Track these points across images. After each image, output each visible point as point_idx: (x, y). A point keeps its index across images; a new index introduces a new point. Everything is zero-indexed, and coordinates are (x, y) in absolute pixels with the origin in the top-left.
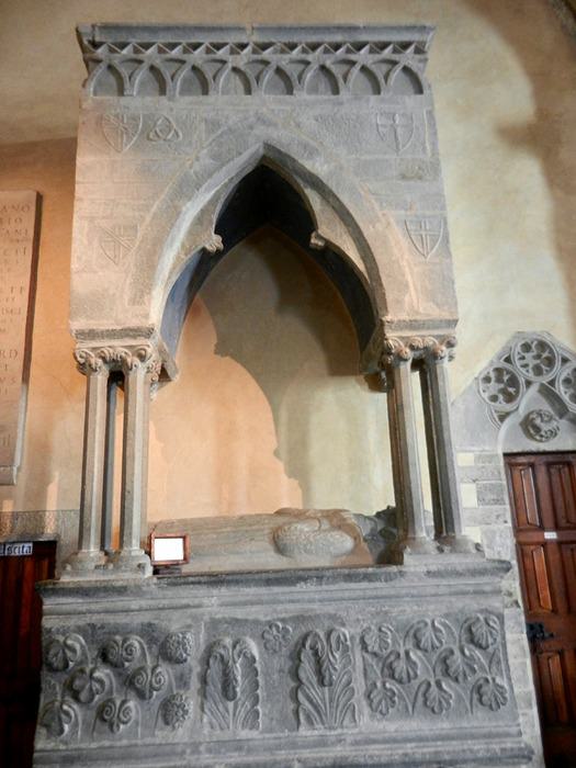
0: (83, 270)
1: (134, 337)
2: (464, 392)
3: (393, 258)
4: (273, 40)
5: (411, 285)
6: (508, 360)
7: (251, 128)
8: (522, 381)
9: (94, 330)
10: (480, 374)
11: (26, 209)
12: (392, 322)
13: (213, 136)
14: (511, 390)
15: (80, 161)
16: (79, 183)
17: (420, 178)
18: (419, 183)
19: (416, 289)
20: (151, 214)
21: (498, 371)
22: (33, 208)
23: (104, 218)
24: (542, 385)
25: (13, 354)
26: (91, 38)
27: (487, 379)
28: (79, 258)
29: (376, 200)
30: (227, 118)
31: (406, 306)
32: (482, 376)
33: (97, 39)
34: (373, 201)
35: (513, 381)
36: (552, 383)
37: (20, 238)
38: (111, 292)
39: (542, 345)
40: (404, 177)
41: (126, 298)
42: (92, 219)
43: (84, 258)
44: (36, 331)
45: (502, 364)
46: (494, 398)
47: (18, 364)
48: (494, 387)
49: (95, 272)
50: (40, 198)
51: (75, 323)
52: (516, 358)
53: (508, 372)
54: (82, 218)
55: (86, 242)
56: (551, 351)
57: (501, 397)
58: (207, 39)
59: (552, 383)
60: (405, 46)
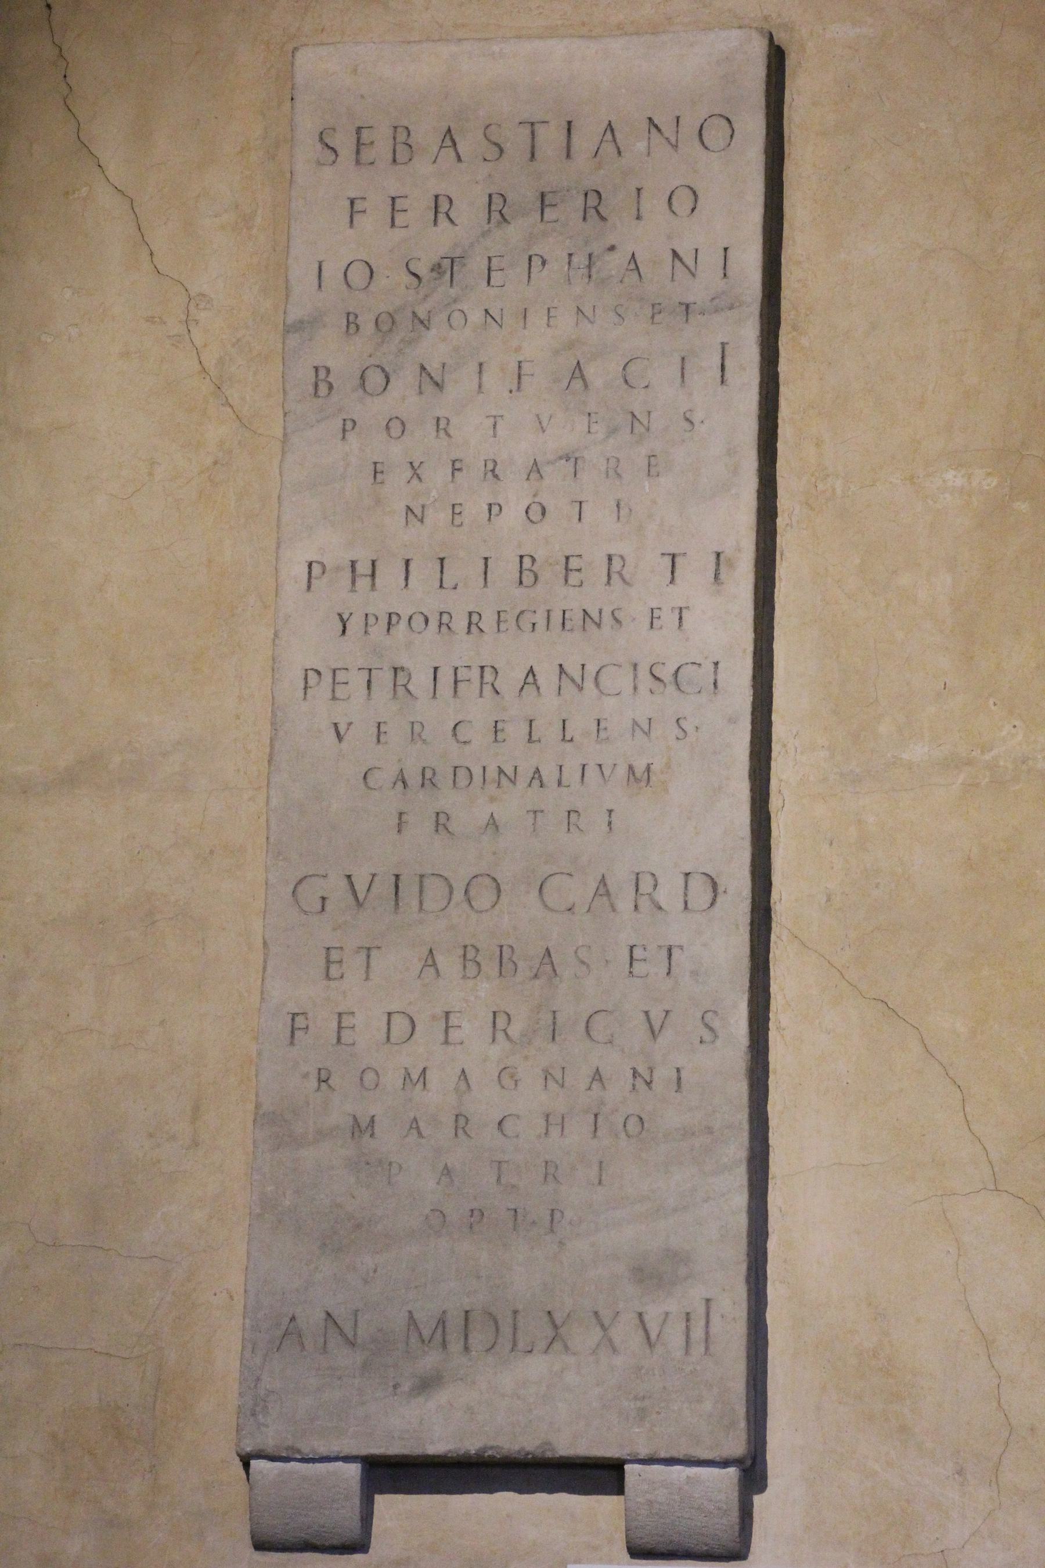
11: (716, 134)
22: (753, 126)
37: (697, 292)
47: (728, 945)
50: (777, 60)
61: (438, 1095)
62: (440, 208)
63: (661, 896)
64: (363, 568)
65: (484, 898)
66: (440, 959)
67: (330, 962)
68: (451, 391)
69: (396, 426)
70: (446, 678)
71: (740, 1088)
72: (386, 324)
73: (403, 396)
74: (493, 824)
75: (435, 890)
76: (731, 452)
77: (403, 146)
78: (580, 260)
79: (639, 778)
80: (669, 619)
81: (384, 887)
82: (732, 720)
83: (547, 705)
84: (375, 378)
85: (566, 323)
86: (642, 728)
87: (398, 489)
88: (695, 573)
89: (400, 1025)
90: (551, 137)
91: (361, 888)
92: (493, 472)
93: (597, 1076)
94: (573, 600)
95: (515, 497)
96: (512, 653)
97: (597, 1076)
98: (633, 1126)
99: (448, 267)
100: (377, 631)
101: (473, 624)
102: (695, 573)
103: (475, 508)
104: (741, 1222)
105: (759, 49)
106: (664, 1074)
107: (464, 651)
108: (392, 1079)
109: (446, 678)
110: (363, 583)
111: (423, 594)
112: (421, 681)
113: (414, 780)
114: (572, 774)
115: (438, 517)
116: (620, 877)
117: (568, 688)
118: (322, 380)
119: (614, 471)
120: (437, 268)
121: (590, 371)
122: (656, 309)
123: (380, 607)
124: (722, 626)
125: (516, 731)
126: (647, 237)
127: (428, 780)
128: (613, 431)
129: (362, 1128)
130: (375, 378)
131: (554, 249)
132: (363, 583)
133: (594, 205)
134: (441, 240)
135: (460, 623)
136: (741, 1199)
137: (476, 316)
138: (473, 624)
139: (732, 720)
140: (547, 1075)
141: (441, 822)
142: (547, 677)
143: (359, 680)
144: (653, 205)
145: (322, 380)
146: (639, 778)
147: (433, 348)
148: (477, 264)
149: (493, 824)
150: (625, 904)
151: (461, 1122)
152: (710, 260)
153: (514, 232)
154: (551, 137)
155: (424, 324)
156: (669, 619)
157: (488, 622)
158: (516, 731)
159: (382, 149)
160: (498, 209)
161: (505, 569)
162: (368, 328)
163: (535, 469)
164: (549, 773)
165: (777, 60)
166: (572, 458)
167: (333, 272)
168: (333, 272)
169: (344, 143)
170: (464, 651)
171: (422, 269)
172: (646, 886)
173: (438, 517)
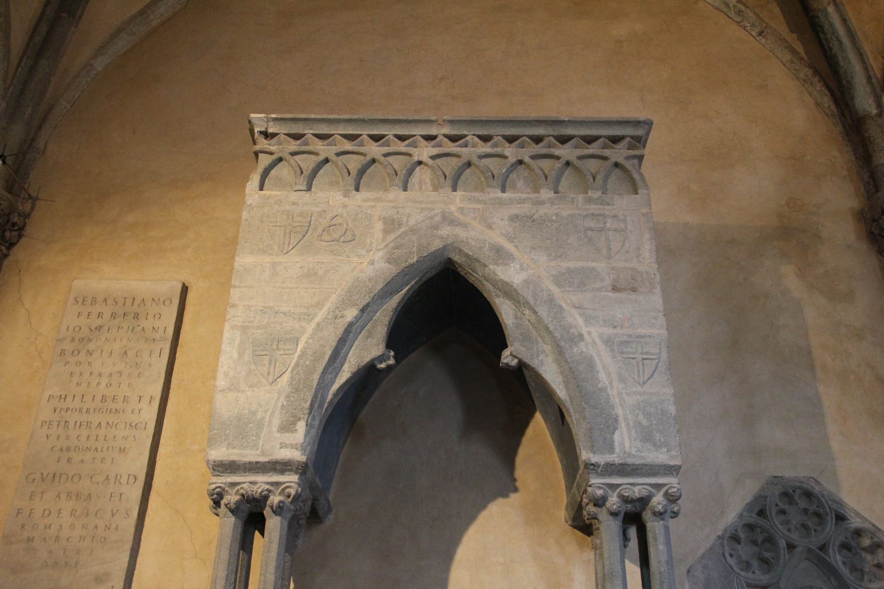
0: (230, 389)
1: (282, 472)
2: (703, 557)
3: (600, 386)
4: (466, 133)
5: (621, 419)
6: (761, 513)
7: (436, 228)
8: (782, 543)
9: (234, 462)
10: (726, 530)
11: (167, 303)
12: (599, 466)
13: (392, 237)
14: (767, 555)
15: (243, 260)
16: (234, 287)
17: (634, 290)
18: (633, 296)
19: (628, 425)
20: (313, 325)
21: (750, 527)
23: (258, 328)
24: (810, 551)
25: (132, 480)
26: (263, 129)
27: (735, 538)
28: (226, 374)
29: (580, 314)
30: (409, 215)
31: (617, 450)
32: (728, 535)
33: (271, 130)
34: (577, 316)
35: (770, 540)
36: (823, 548)
37: (157, 336)
38: (259, 415)
39: (808, 495)
40: (615, 289)
41: (276, 422)
42: (244, 329)
43: (232, 374)
44: (161, 450)
45: (754, 519)
46: (747, 566)
47: (136, 493)
48: (745, 551)
49: (243, 391)
50: (185, 290)
51: (213, 452)
52: (774, 512)
53: (763, 530)
54: (234, 327)
55: (235, 355)
56: (820, 505)
57: (755, 564)
58: (389, 131)
59: (823, 548)
60: (615, 140)
61: (53, 531)
62: (100, 315)
63: (122, 481)
64: (63, 397)
65: (76, 479)
66: (61, 495)
67: (32, 496)
68: (94, 356)
69: (78, 364)
70: (78, 424)
71: (132, 531)
72: (81, 340)
73: (82, 356)
74: (82, 461)
75: (64, 477)
76: (159, 373)
77: (94, 301)
78: (131, 328)
79: (122, 450)
80: (137, 411)
81: (51, 476)
82: (148, 437)
83: (102, 432)
84: (76, 352)
85: (125, 342)
86: (125, 438)
87: (76, 379)
88: (146, 401)
89: (47, 512)
90: (129, 302)
91: (45, 476)
92: (100, 375)
93: (96, 527)
94: (114, 406)
95: (104, 381)
96: (95, 419)
97: (96, 527)
98: (102, 540)
99: (99, 328)
100: (63, 412)
101: (88, 411)
102: (146, 401)
103: (94, 384)
104: (125, 565)
105: (180, 286)
106: (113, 526)
107: (84, 418)
108: (41, 527)
109: (78, 424)
110: (62, 400)
111: (77, 404)
112: (72, 424)
113: (64, 449)
114: (105, 449)
115: (84, 385)
116: (112, 476)
117: (109, 428)
118: (63, 352)
119: (130, 376)
120: (96, 328)
121: (128, 352)
122: (147, 340)
123: (65, 406)
124: (150, 414)
125: (93, 438)
126: (148, 324)
127: (68, 449)
128: (131, 367)
129: (30, 540)
130: (76, 352)
131: (125, 325)
132: (62, 400)
133: (136, 316)
134: (99, 322)
135: (84, 411)
136: (127, 559)
137: (103, 339)
138: (88, 411)
139: (148, 437)
140: (83, 526)
141: (69, 460)
142: (104, 425)
143: (56, 424)
144: (150, 317)
145: (63, 352)
146: (122, 450)
147: (91, 346)
148: (106, 328)
149: (82, 461)
150: (112, 481)
151: (57, 538)
152: (161, 330)
153: (116, 321)
154: (129, 302)
155: (91, 340)
156: (137, 411)
157: (92, 411)
158: (93, 438)
159: (89, 302)
160: (113, 316)
161: (98, 398)
162: (77, 341)
163: (111, 375)
164: (99, 449)
165: (185, 290)
166: (120, 373)
167: (71, 328)
168: (71, 328)
169: (80, 300)
170: (84, 418)
171: (93, 328)
172: (118, 478)
173: (84, 385)
